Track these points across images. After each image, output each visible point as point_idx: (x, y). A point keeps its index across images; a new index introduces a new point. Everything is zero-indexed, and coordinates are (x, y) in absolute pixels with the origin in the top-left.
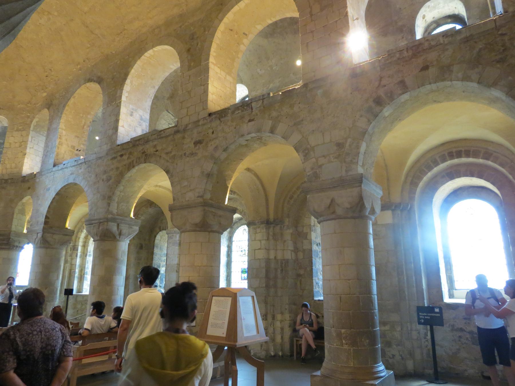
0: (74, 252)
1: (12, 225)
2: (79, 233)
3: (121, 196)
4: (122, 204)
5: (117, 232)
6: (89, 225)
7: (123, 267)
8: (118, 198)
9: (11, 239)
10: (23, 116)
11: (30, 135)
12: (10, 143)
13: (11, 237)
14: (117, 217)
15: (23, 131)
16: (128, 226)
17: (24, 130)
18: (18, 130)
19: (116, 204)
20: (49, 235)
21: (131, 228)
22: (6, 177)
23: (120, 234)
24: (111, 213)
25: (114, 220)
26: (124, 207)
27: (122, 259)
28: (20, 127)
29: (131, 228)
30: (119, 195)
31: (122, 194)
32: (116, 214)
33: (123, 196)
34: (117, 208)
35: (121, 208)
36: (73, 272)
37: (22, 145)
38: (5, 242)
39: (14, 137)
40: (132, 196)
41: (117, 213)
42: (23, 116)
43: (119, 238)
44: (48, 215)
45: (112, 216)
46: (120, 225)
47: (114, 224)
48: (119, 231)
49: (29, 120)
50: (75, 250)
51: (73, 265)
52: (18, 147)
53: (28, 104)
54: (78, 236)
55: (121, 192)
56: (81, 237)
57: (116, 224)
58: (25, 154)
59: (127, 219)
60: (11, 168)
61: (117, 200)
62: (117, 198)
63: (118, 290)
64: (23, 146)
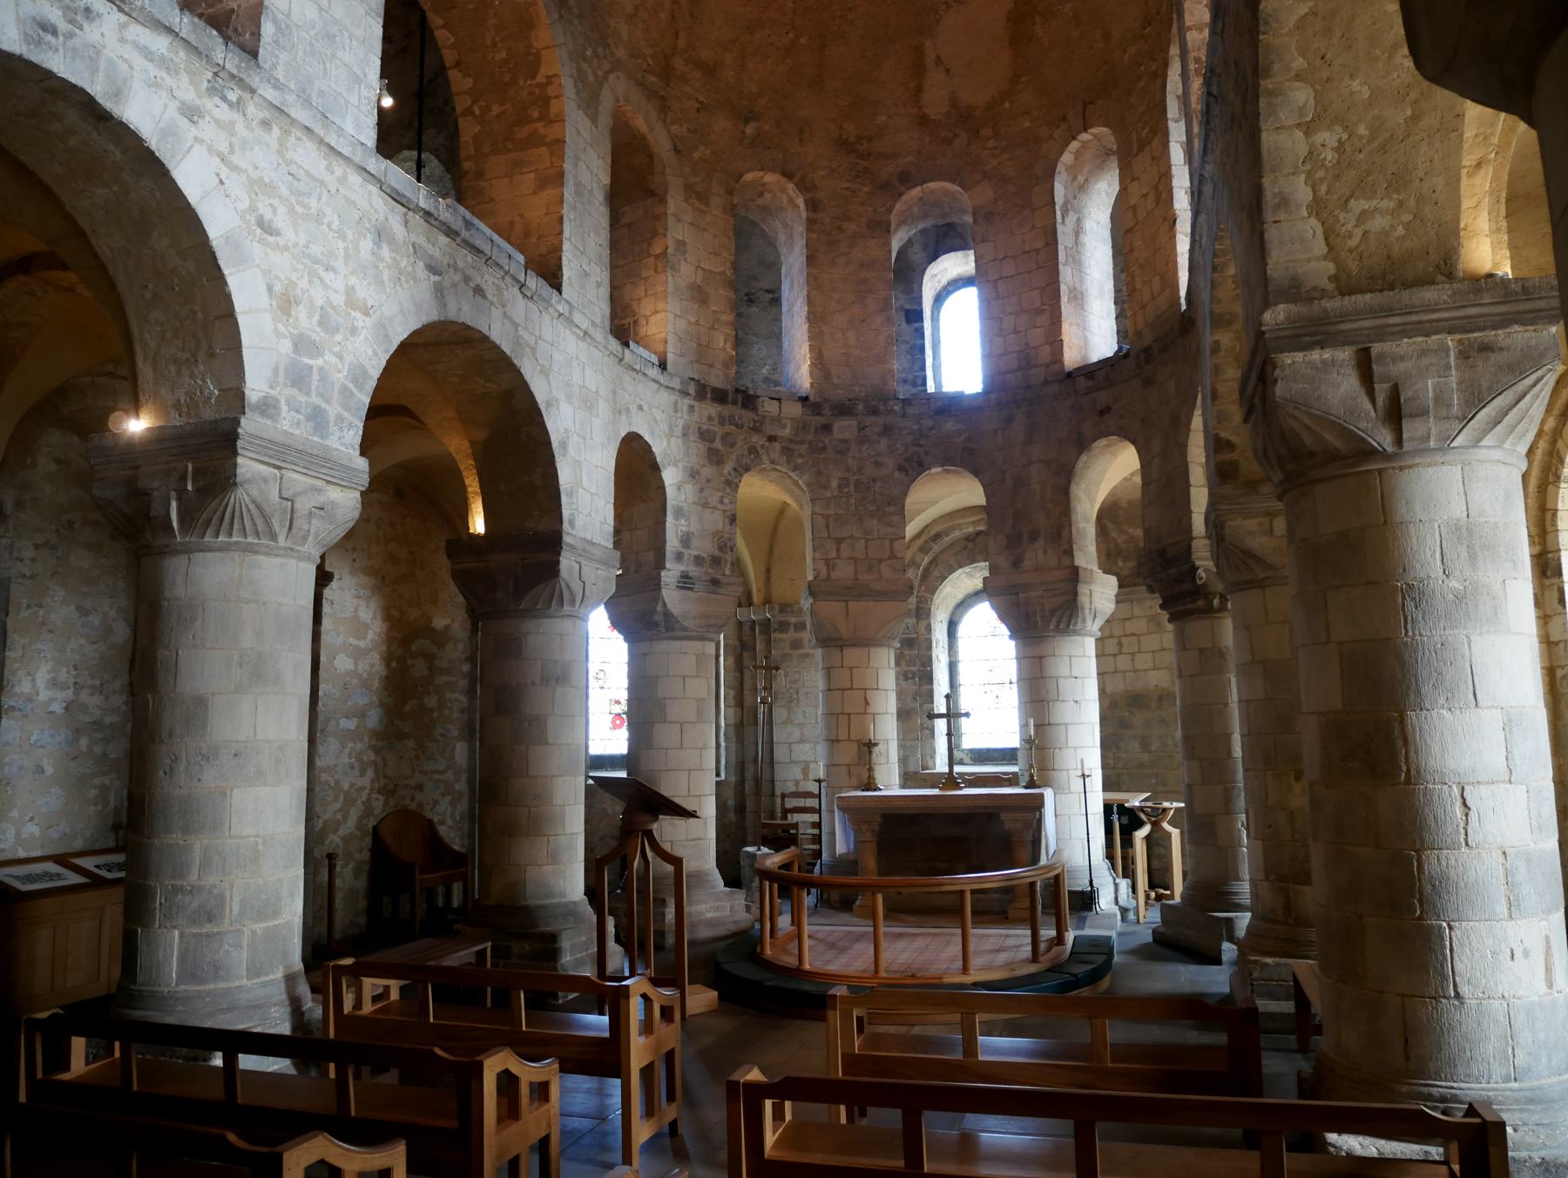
0: (1547, 582)
1: (1191, 512)
2: (1550, 488)
3: (1329, 156)
4: (1358, 205)
5: (1368, 405)
6: (1511, 432)
7: (1475, 639)
8: (1309, 174)
9: (1199, 571)
10: (1142, 84)
11: (1171, 139)
12: (1134, 209)
13: (1198, 563)
14: (1333, 304)
15: (1152, 139)
16: (1450, 341)
17: (1154, 132)
18: (1141, 149)
19: (1314, 222)
20: (1252, 524)
21: (1486, 348)
22: (1148, 339)
23: (1395, 415)
24: (1295, 291)
25: (1317, 333)
26: (1378, 223)
27: (1454, 583)
28: (1144, 134)
29: (1486, 348)
30: (1311, 153)
31: (1327, 138)
32: (1330, 286)
33: (1340, 148)
34: (1327, 244)
35: (1358, 233)
36: (1564, 677)
37: (1160, 194)
38: (1187, 587)
39: (1138, 178)
40: (1415, 119)
41: (1334, 278)
42: (1142, 84)
43: (1399, 441)
44: (1223, 435)
45: (1293, 308)
46: (1376, 349)
47: (1327, 354)
48: (1381, 398)
49: (1159, 81)
50: (1549, 574)
51: (1557, 643)
52: (1153, 210)
53: (1145, 28)
54: (1549, 505)
55: (1308, 129)
56: (1560, 506)
57: (1345, 354)
58: (1175, 220)
59: (1428, 295)
60: (1153, 299)
61: (1302, 192)
62: (1303, 177)
63: (1467, 815)
64: (1164, 196)
